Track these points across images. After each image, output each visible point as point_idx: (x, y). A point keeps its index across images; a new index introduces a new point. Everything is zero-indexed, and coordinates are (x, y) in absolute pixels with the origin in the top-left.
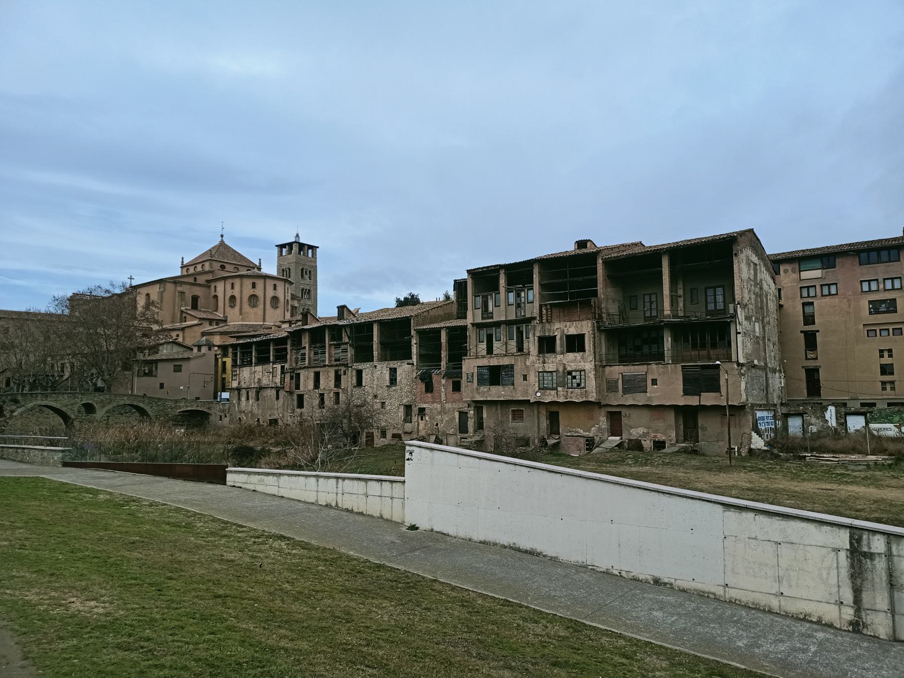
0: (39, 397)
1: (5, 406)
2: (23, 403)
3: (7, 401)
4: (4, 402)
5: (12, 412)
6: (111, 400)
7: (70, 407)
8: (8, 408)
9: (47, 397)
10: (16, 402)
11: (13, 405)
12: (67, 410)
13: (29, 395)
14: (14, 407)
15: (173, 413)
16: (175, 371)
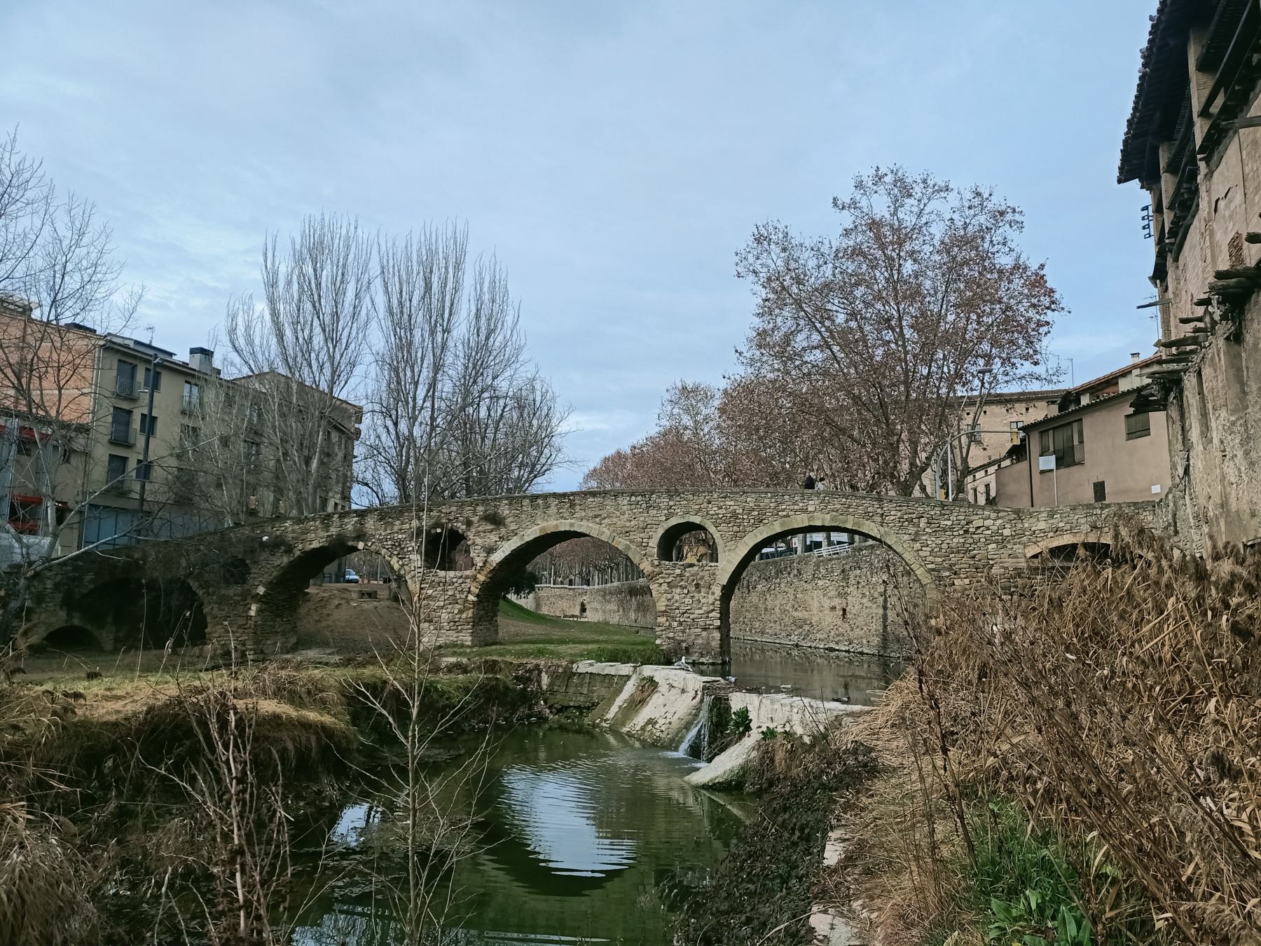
0: (553, 510)
1: (470, 535)
2: (513, 527)
3: (475, 519)
4: (469, 523)
5: (490, 550)
6: (762, 512)
7: (638, 537)
8: (479, 541)
9: (572, 505)
10: (496, 520)
11: (492, 531)
12: (628, 548)
13: (526, 502)
14: (493, 537)
15: (1010, 563)
16: (1132, 435)
